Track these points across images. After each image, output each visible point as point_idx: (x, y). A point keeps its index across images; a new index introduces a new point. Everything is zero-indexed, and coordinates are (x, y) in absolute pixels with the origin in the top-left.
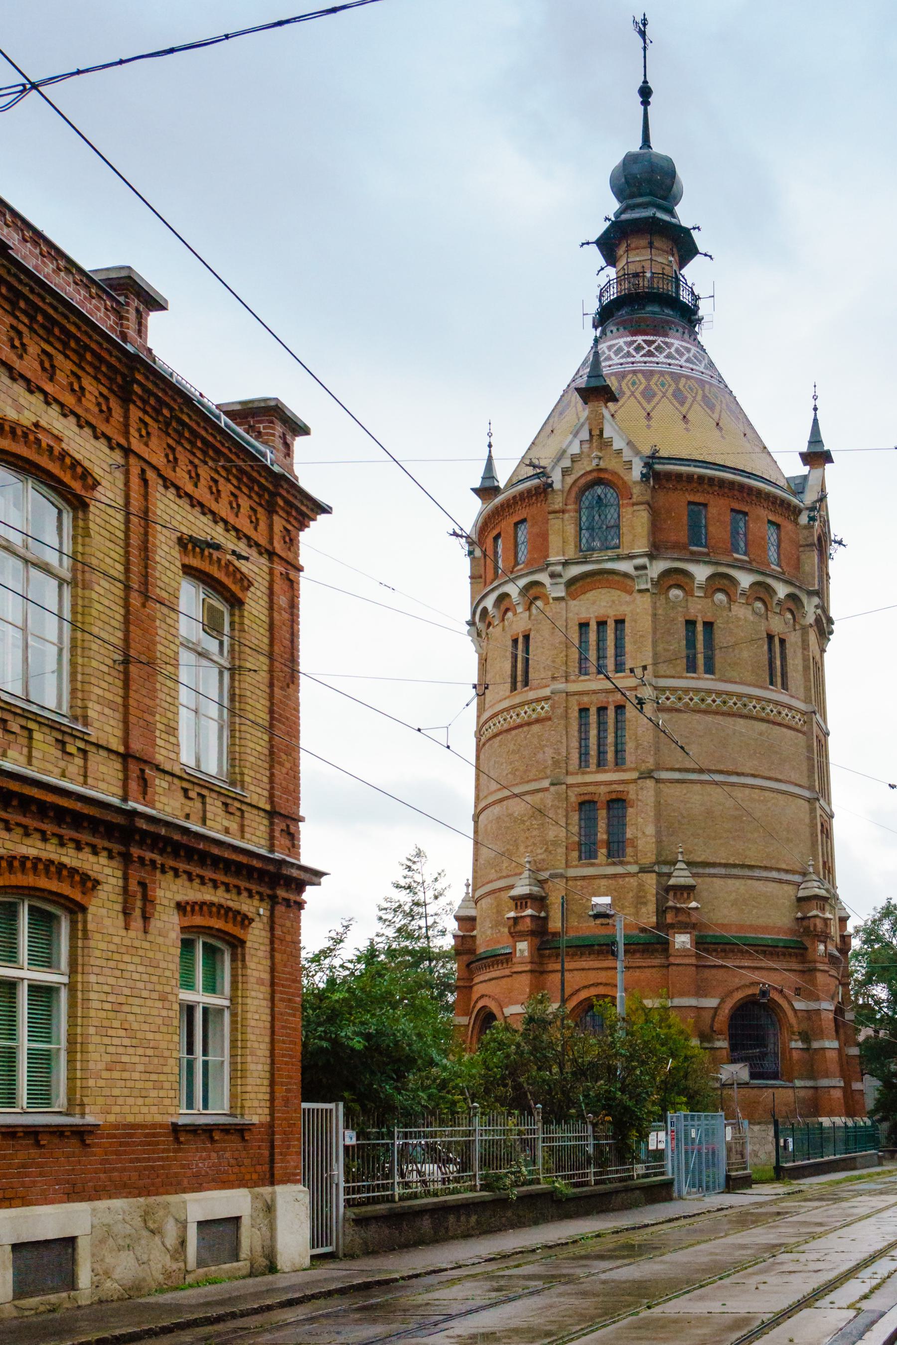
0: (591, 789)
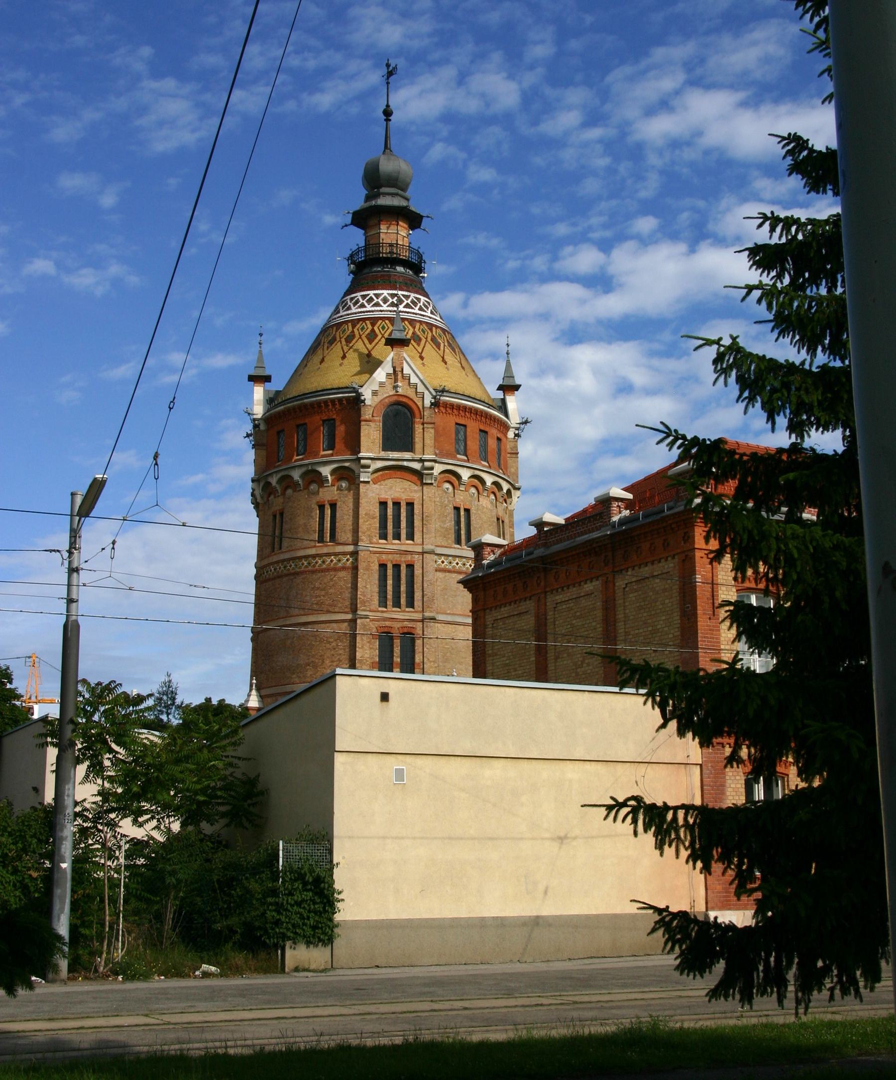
0: (388, 623)
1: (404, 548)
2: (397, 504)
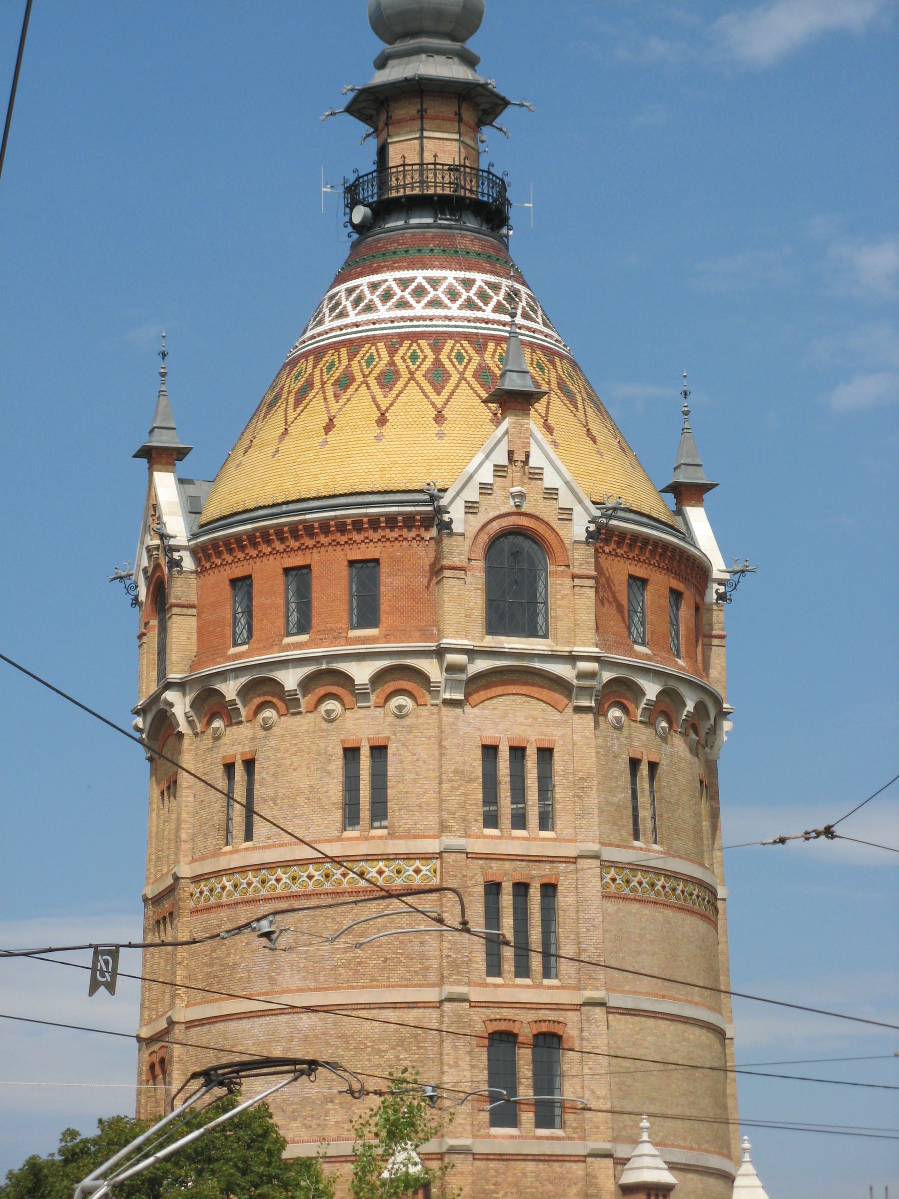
0: (506, 1013)
1: (535, 850)
2: (518, 752)
